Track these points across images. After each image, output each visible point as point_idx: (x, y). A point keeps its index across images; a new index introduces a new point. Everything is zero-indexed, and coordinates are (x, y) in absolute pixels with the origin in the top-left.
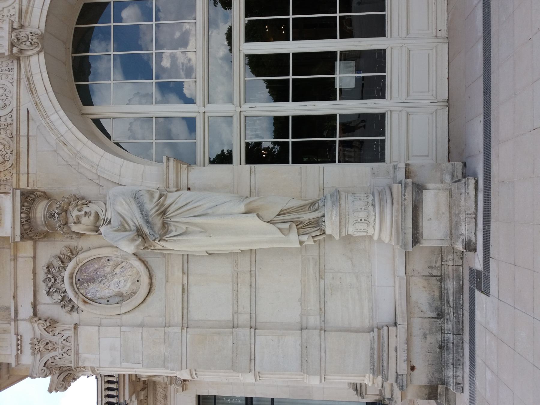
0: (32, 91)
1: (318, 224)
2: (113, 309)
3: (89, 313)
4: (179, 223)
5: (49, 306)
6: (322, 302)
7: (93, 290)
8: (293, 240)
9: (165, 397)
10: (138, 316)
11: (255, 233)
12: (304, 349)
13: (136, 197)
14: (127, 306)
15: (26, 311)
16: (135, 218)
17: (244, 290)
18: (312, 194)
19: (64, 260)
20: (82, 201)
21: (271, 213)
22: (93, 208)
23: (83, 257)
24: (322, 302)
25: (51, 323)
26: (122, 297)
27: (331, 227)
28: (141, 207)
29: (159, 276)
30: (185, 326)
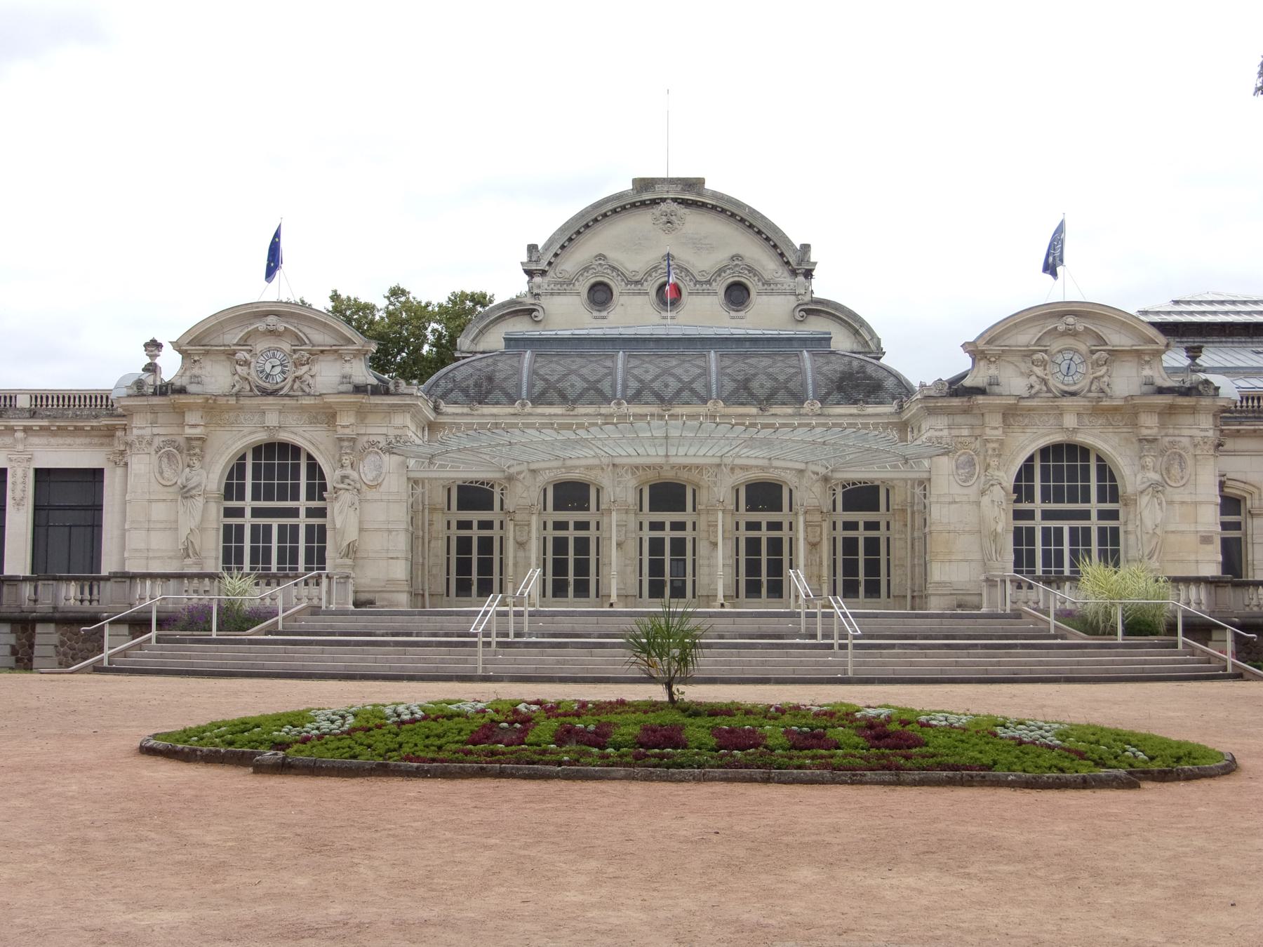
0: (251, 433)
1: (188, 556)
2: (156, 470)
3: (155, 458)
4: (189, 502)
5: (158, 441)
6: (158, 558)
7: (165, 460)
8: (181, 547)
9: (102, 444)
10: (153, 480)
11: (184, 532)
12: (140, 550)
13: (199, 485)
14: (158, 475)
15: (156, 431)
16: (191, 484)
17: (162, 526)
18: (203, 554)
19: (177, 448)
20: (201, 457)
21: (191, 538)
22: (197, 464)
23: (179, 457)
24: (158, 558)
25: (150, 443)
26: (161, 473)
27: (188, 561)
28: (193, 488)
29: (170, 489)
30: (150, 501)
